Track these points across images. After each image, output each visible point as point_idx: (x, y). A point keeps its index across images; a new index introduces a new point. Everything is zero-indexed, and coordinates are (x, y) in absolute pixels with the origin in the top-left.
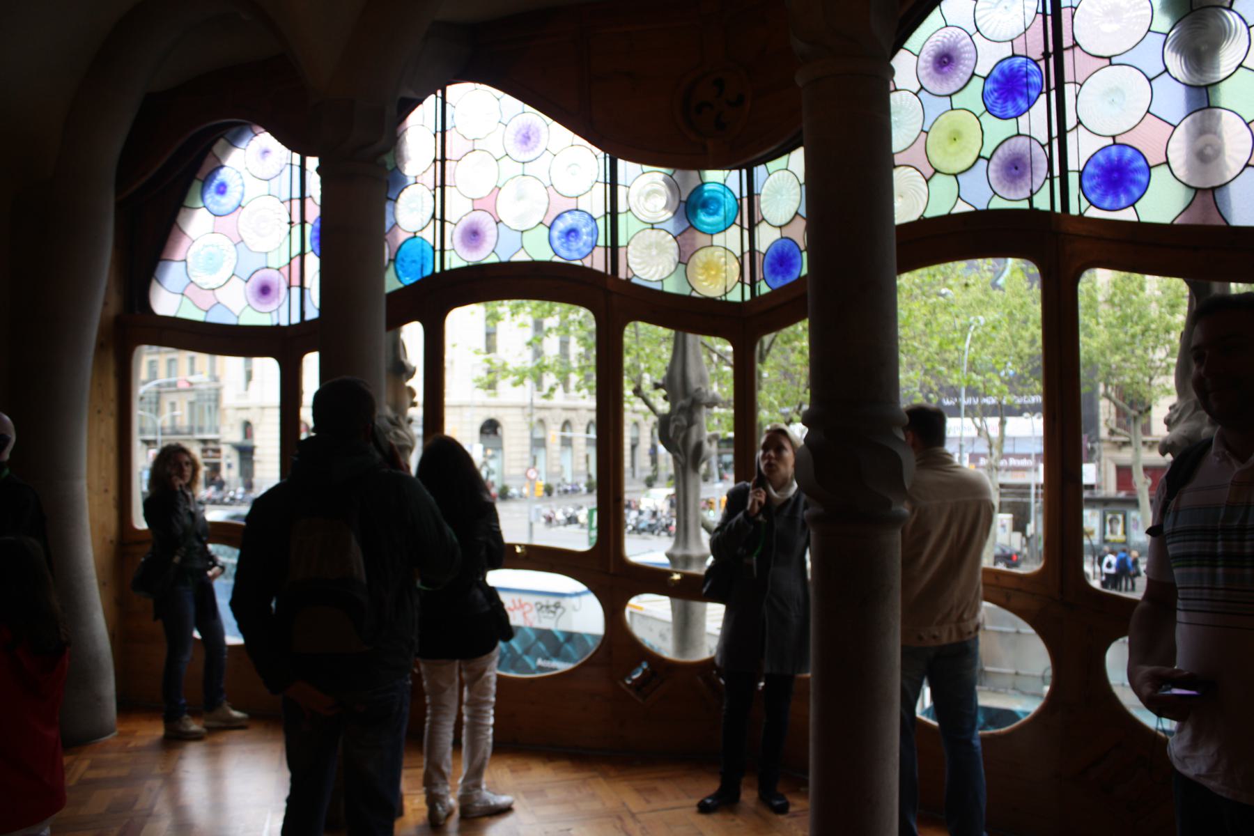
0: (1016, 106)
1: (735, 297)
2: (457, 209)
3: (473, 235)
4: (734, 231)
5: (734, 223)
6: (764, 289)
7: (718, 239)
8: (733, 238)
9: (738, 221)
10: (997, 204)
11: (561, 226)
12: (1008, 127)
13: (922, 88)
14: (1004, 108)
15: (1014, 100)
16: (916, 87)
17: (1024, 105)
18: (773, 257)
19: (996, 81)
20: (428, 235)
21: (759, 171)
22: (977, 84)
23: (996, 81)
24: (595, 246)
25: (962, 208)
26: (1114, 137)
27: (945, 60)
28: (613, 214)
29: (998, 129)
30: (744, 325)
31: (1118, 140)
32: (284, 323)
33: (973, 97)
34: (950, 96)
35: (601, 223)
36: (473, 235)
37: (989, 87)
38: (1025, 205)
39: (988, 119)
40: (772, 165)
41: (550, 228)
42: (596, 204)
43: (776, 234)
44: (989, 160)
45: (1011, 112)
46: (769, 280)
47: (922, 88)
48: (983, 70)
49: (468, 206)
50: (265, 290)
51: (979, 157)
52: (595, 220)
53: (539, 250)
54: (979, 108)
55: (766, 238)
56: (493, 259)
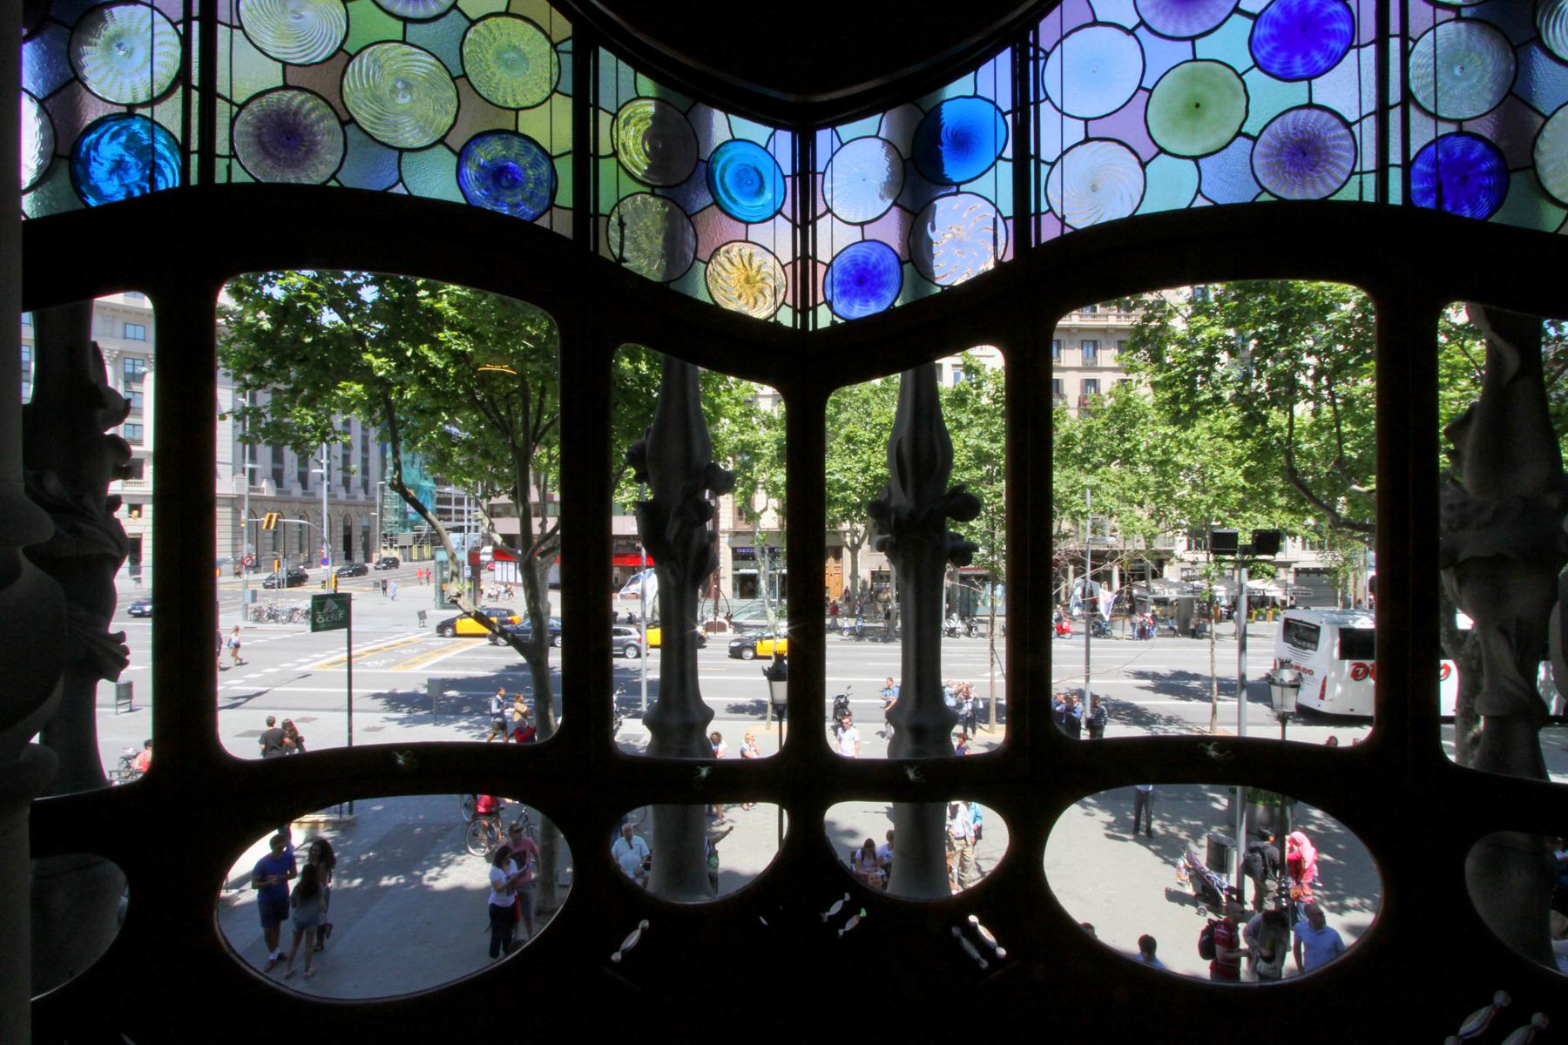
0: (1308, 63)
1: (786, 318)
4: (784, 228)
5: (779, 212)
6: (824, 318)
7: (756, 232)
8: (780, 236)
9: (787, 210)
11: (485, 154)
12: (1296, 93)
13: (1142, 23)
15: (1306, 55)
16: (1131, 21)
17: (1322, 63)
18: (844, 271)
19: (1274, 23)
24: (552, 205)
26: (1459, 122)
28: (584, 152)
29: (1271, 97)
30: (806, 365)
31: (1467, 127)
34: (1193, 39)
35: (565, 169)
36: (283, 134)
37: (1263, 31)
39: (1256, 78)
40: (846, 131)
41: (462, 155)
42: (551, 126)
43: (854, 235)
44: (1255, 139)
46: (838, 307)
47: (1142, 23)
51: (1239, 134)
52: (551, 158)
53: (436, 181)
54: (1243, 60)
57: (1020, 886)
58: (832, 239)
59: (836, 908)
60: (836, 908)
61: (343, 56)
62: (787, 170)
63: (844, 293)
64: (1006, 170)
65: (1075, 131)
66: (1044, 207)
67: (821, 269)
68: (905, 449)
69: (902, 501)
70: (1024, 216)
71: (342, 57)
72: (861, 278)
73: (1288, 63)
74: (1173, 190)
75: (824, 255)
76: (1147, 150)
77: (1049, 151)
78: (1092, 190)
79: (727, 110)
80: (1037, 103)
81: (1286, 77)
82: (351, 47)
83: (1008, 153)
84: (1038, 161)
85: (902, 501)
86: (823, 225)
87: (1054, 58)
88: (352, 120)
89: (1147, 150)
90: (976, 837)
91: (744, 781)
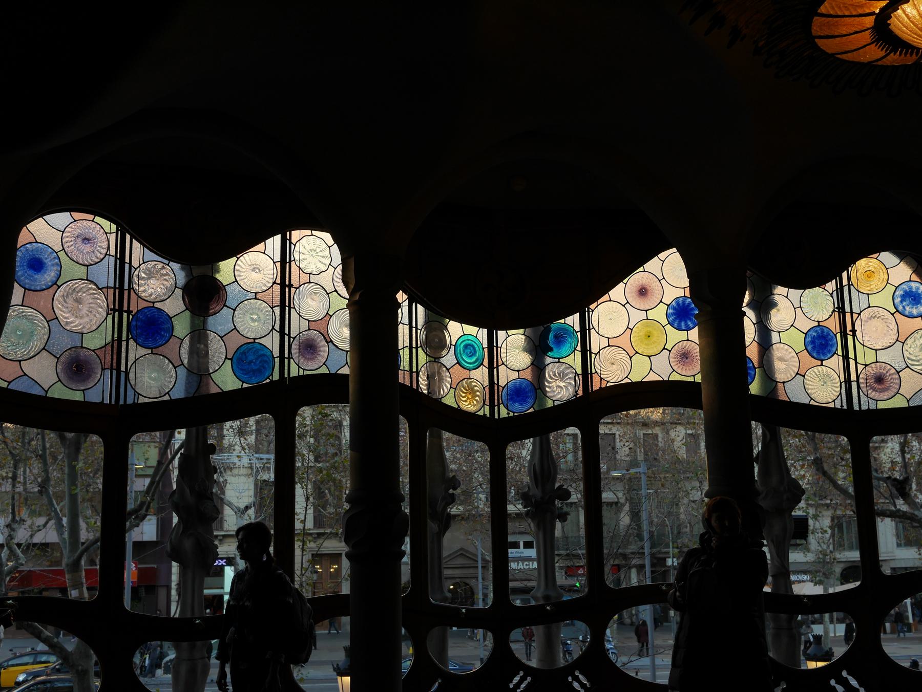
0: (687, 325)
2: (297, 326)
3: (309, 348)
6: (504, 413)
7: (474, 374)
9: (486, 362)
10: (675, 377)
12: (683, 335)
14: (679, 325)
15: (686, 322)
18: (511, 390)
19: (674, 308)
20: (272, 343)
21: (501, 334)
22: (663, 308)
23: (674, 308)
25: (653, 377)
27: (643, 292)
32: (107, 401)
33: (660, 314)
37: (670, 311)
38: (691, 379)
39: (668, 328)
43: (515, 375)
45: (683, 327)
48: (668, 299)
49: (304, 325)
50: (76, 367)
51: (664, 348)
55: (505, 377)
56: (323, 370)
57: (595, 659)
58: (505, 377)
59: (517, 679)
60: (517, 679)
61: (329, 316)
62: (485, 345)
63: (511, 399)
64: (578, 355)
65: (604, 342)
66: (594, 371)
67: (501, 389)
68: (537, 468)
69: (536, 492)
70: (586, 374)
71: (328, 317)
72: (518, 393)
73: (679, 325)
74: (640, 372)
75: (502, 383)
76: (632, 352)
77: (595, 349)
78: (612, 370)
79: (462, 320)
80: (589, 329)
81: (679, 329)
82: (331, 313)
83: (579, 348)
84: (591, 353)
85: (536, 492)
86: (502, 369)
87: (595, 312)
88: (331, 341)
89: (632, 352)
90: (574, 638)
91: (475, 620)
